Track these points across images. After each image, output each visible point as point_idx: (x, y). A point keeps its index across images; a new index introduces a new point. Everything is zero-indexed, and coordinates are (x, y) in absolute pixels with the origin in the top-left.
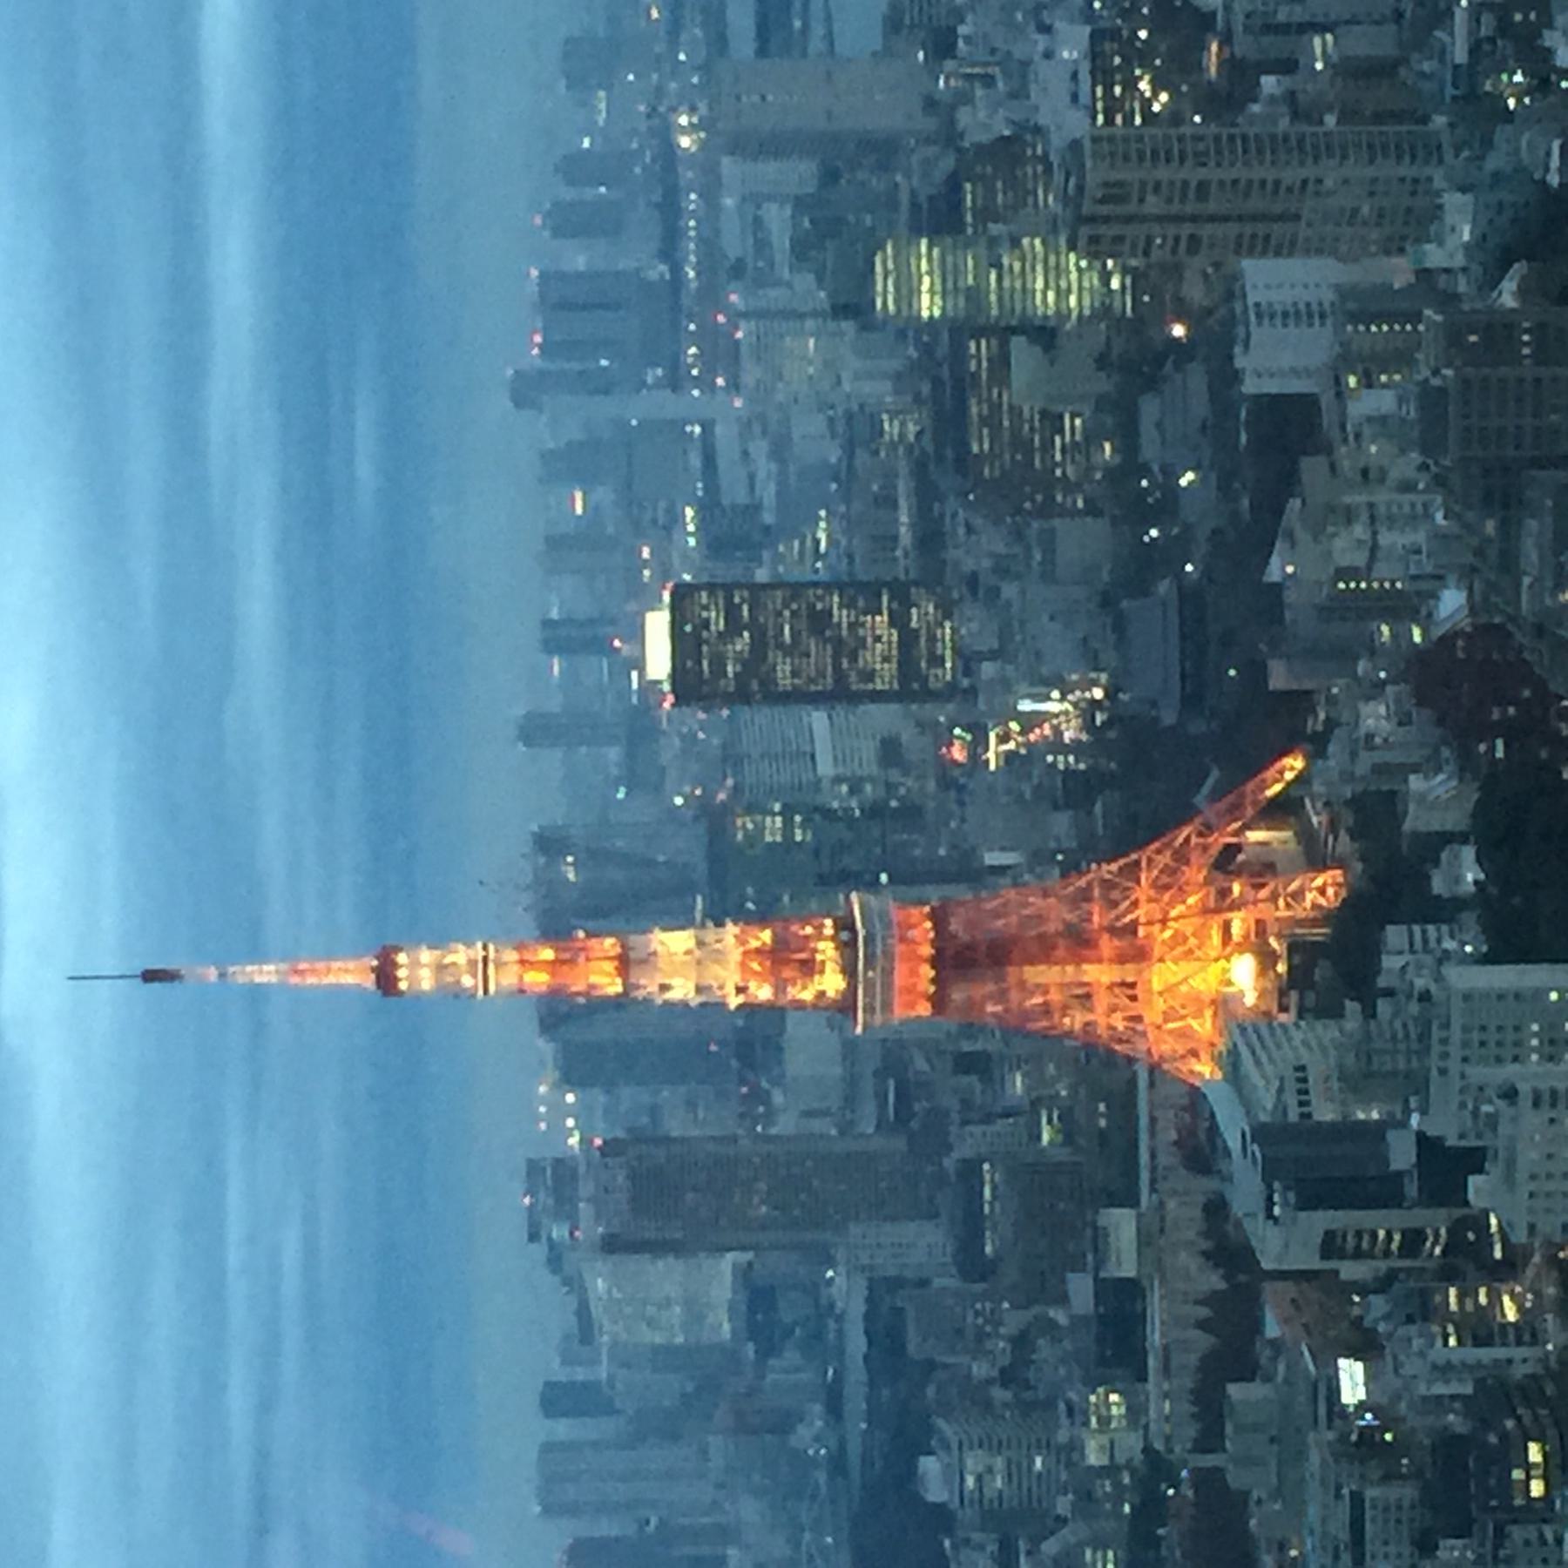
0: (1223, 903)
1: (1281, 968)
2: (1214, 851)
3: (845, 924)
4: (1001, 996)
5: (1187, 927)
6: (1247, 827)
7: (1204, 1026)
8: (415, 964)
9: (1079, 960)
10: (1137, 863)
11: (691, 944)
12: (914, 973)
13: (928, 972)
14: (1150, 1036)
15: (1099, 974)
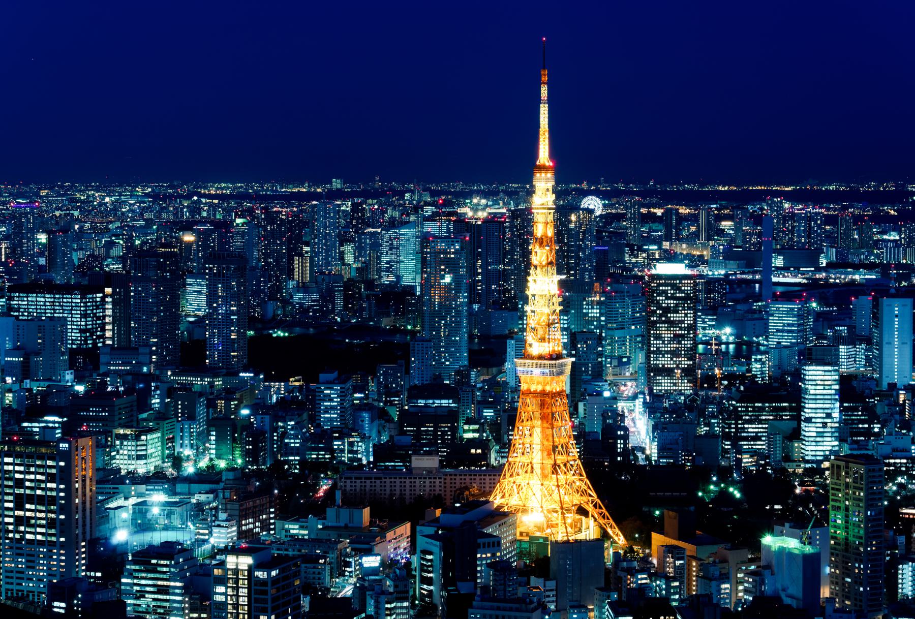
1: (538, 534)
2: (586, 507)
3: (559, 356)
6: (595, 520)
8: (547, 180)
9: (542, 451)
10: (581, 475)
12: (538, 383)
13: (539, 388)
15: (537, 457)
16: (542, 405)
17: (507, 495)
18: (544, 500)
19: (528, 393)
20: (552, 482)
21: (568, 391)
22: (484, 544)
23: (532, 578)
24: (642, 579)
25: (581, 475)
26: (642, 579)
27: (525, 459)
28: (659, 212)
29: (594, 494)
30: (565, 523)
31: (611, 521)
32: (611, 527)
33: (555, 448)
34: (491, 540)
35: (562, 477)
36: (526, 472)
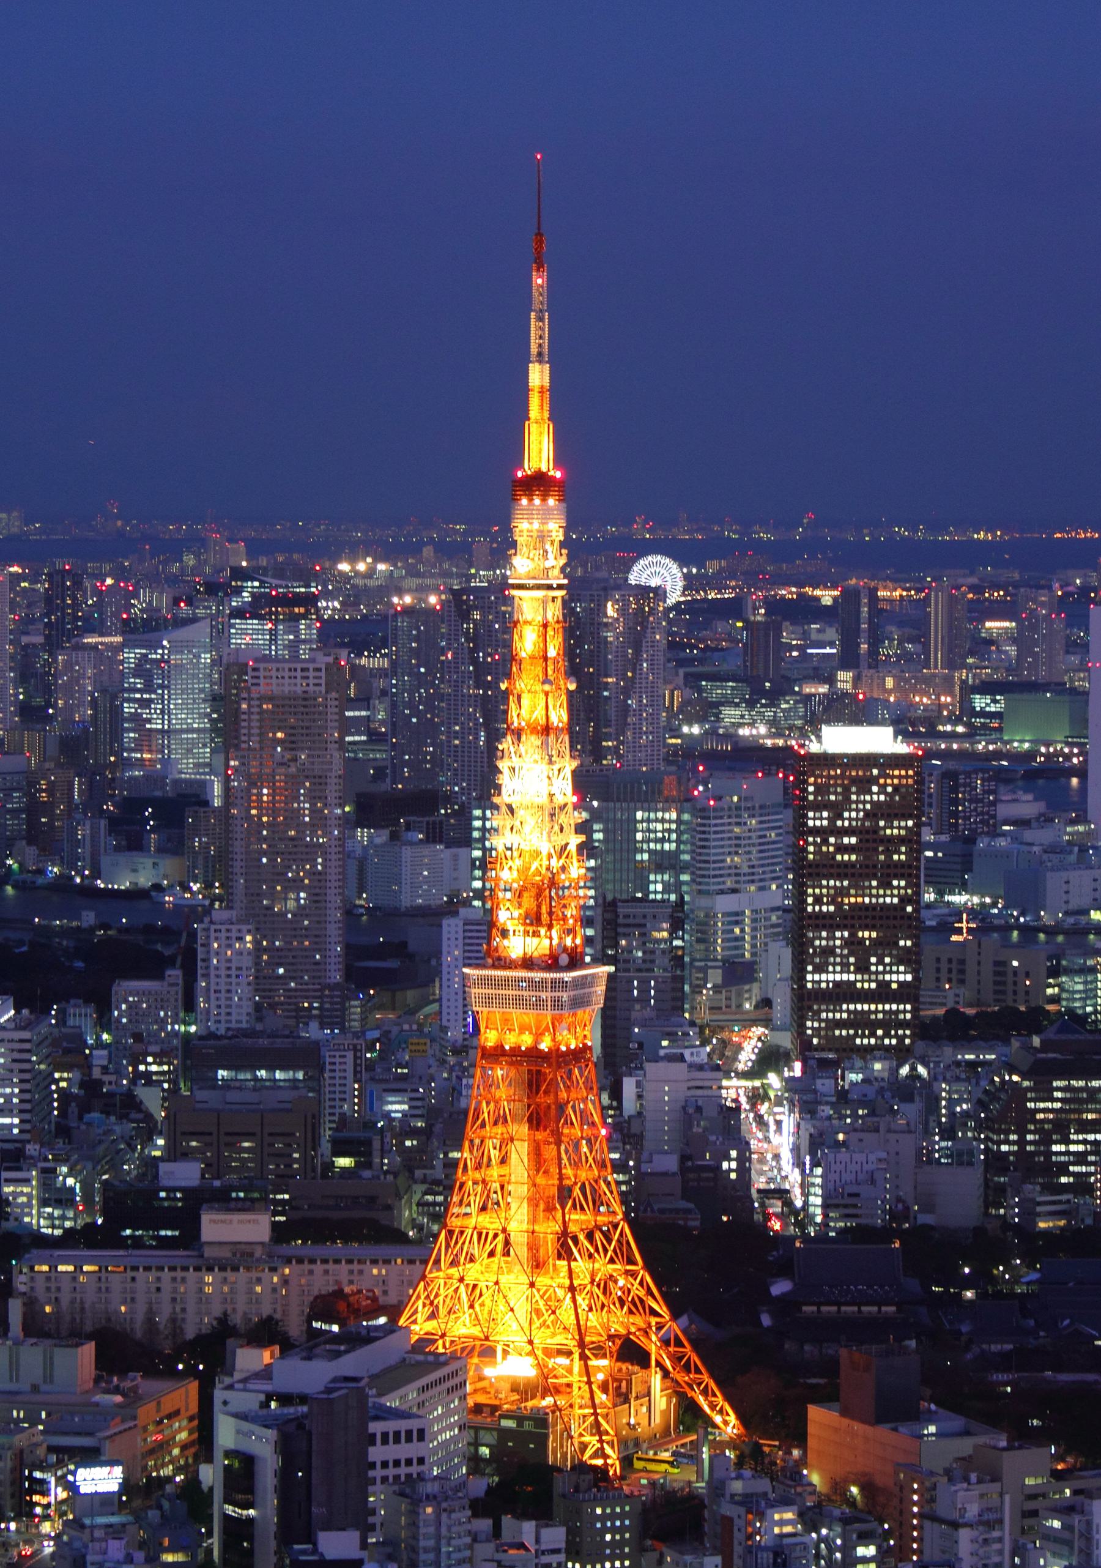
0: (585, 1349)
2: (642, 1341)
4: (500, 1119)
5: (567, 1316)
6: (666, 1374)
7: (462, 1327)
9: (533, 1202)
10: (631, 1261)
11: (560, 800)
12: (523, 1029)
14: (453, 1271)
15: (518, 1219)
16: (534, 1084)
17: (442, 1311)
18: (537, 1323)
19: (497, 1054)
20: (554, 1279)
21: (597, 1051)
22: (385, 1435)
23: (507, 1520)
24: (782, 1523)
25: (631, 1261)
26: (782, 1523)
27: (489, 1222)
28: (827, 596)
29: (663, 1310)
30: (589, 1383)
31: (706, 1378)
32: (705, 1392)
33: (564, 1193)
34: (402, 1425)
35: (581, 1266)
36: (492, 1254)
